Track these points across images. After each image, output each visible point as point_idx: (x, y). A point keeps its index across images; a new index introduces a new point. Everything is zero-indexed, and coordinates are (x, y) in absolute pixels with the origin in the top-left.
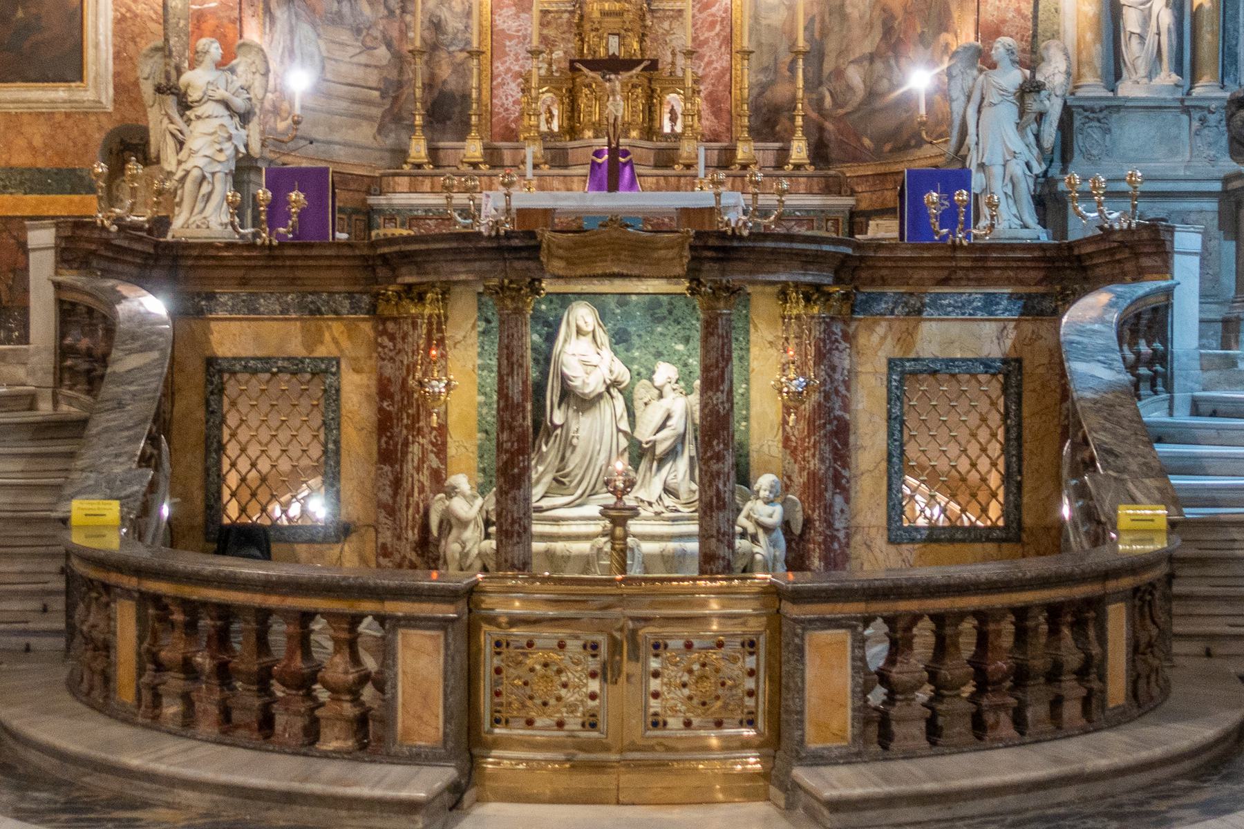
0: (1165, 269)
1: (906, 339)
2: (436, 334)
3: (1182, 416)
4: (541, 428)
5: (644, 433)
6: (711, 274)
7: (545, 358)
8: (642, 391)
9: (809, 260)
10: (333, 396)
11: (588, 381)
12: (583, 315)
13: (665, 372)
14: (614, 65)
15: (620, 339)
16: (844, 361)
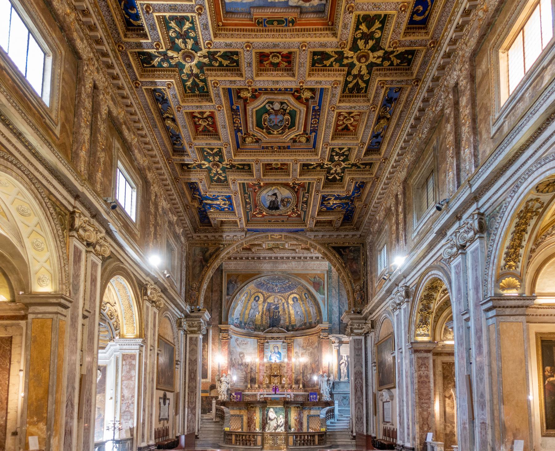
0: (334, 405)
1: (309, 412)
2: (255, 412)
3: (336, 421)
4: (267, 423)
5: (279, 424)
6: (286, 405)
7: (267, 415)
8: (278, 419)
9: (297, 404)
10: (242, 419)
11: (272, 417)
12: (272, 410)
13: (281, 416)
14: (275, 376)
15: (276, 412)
16: (302, 415)
